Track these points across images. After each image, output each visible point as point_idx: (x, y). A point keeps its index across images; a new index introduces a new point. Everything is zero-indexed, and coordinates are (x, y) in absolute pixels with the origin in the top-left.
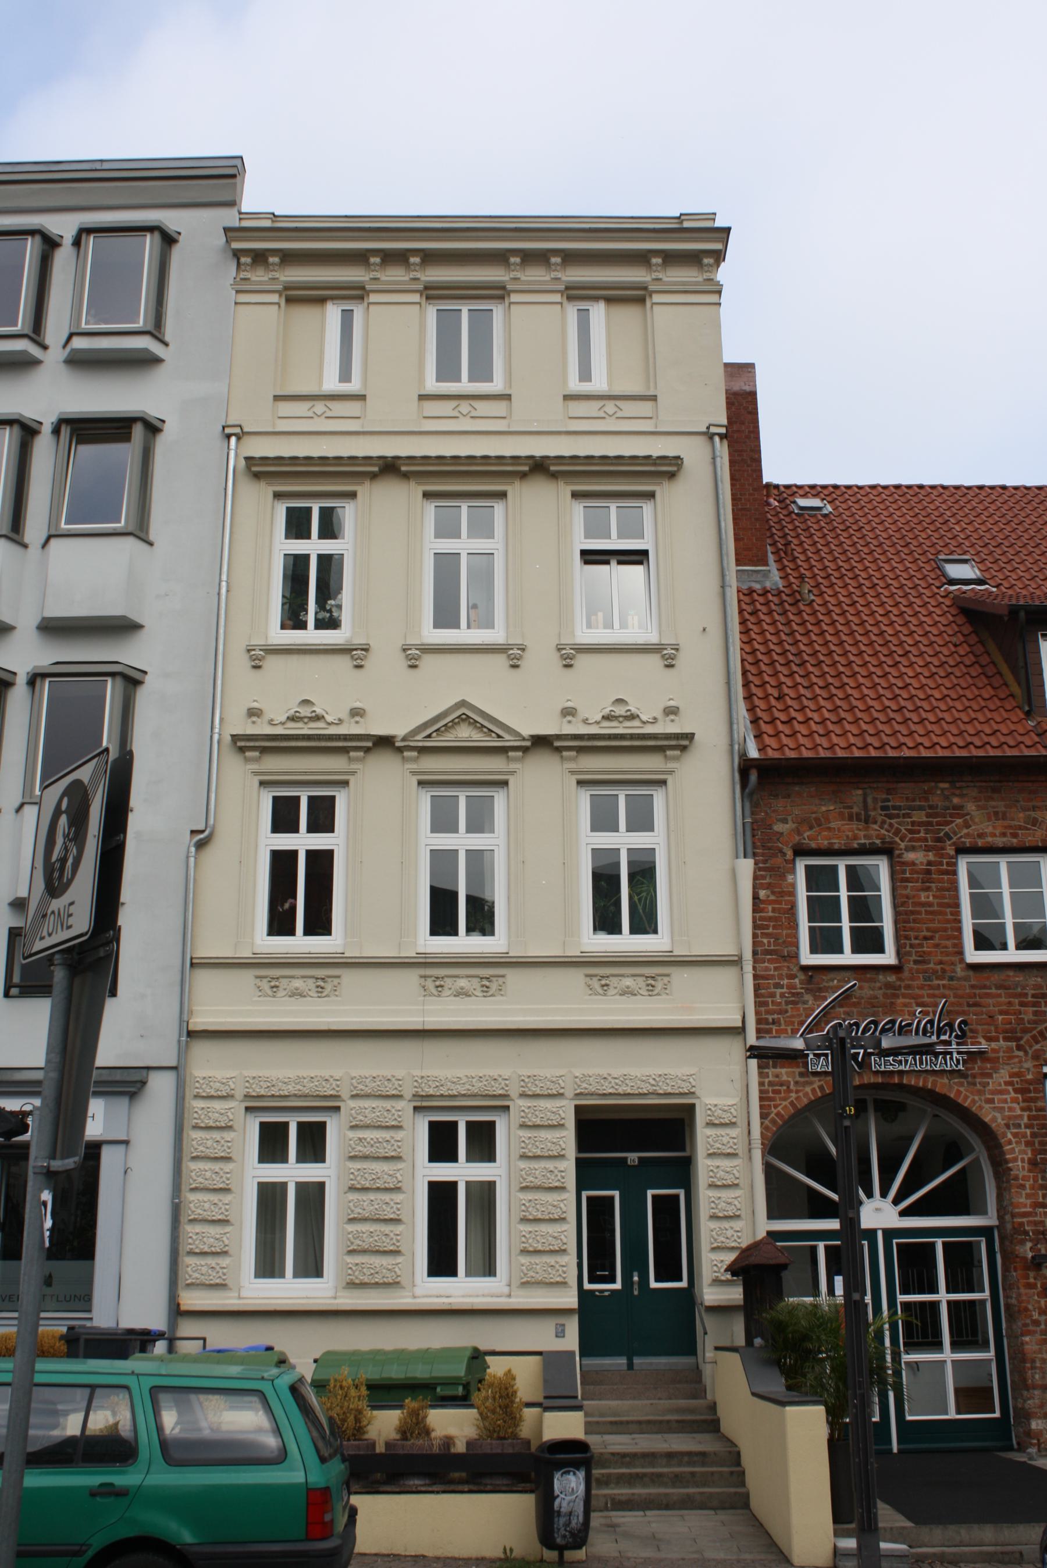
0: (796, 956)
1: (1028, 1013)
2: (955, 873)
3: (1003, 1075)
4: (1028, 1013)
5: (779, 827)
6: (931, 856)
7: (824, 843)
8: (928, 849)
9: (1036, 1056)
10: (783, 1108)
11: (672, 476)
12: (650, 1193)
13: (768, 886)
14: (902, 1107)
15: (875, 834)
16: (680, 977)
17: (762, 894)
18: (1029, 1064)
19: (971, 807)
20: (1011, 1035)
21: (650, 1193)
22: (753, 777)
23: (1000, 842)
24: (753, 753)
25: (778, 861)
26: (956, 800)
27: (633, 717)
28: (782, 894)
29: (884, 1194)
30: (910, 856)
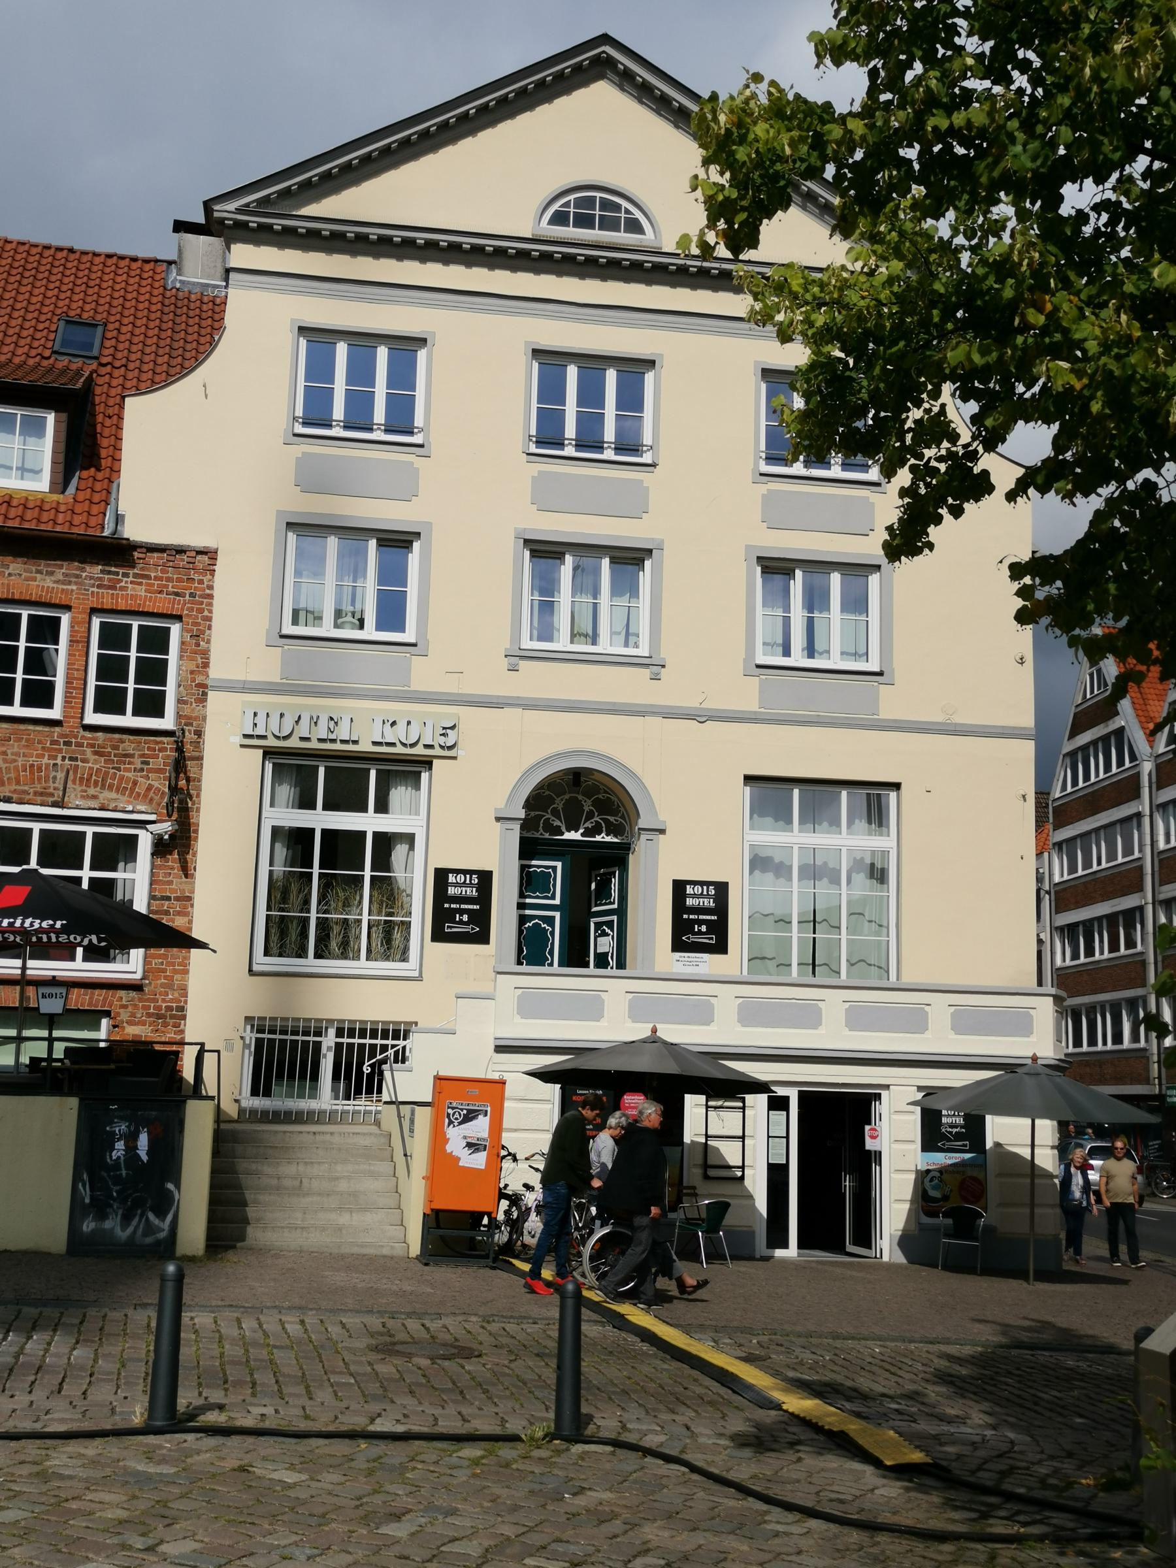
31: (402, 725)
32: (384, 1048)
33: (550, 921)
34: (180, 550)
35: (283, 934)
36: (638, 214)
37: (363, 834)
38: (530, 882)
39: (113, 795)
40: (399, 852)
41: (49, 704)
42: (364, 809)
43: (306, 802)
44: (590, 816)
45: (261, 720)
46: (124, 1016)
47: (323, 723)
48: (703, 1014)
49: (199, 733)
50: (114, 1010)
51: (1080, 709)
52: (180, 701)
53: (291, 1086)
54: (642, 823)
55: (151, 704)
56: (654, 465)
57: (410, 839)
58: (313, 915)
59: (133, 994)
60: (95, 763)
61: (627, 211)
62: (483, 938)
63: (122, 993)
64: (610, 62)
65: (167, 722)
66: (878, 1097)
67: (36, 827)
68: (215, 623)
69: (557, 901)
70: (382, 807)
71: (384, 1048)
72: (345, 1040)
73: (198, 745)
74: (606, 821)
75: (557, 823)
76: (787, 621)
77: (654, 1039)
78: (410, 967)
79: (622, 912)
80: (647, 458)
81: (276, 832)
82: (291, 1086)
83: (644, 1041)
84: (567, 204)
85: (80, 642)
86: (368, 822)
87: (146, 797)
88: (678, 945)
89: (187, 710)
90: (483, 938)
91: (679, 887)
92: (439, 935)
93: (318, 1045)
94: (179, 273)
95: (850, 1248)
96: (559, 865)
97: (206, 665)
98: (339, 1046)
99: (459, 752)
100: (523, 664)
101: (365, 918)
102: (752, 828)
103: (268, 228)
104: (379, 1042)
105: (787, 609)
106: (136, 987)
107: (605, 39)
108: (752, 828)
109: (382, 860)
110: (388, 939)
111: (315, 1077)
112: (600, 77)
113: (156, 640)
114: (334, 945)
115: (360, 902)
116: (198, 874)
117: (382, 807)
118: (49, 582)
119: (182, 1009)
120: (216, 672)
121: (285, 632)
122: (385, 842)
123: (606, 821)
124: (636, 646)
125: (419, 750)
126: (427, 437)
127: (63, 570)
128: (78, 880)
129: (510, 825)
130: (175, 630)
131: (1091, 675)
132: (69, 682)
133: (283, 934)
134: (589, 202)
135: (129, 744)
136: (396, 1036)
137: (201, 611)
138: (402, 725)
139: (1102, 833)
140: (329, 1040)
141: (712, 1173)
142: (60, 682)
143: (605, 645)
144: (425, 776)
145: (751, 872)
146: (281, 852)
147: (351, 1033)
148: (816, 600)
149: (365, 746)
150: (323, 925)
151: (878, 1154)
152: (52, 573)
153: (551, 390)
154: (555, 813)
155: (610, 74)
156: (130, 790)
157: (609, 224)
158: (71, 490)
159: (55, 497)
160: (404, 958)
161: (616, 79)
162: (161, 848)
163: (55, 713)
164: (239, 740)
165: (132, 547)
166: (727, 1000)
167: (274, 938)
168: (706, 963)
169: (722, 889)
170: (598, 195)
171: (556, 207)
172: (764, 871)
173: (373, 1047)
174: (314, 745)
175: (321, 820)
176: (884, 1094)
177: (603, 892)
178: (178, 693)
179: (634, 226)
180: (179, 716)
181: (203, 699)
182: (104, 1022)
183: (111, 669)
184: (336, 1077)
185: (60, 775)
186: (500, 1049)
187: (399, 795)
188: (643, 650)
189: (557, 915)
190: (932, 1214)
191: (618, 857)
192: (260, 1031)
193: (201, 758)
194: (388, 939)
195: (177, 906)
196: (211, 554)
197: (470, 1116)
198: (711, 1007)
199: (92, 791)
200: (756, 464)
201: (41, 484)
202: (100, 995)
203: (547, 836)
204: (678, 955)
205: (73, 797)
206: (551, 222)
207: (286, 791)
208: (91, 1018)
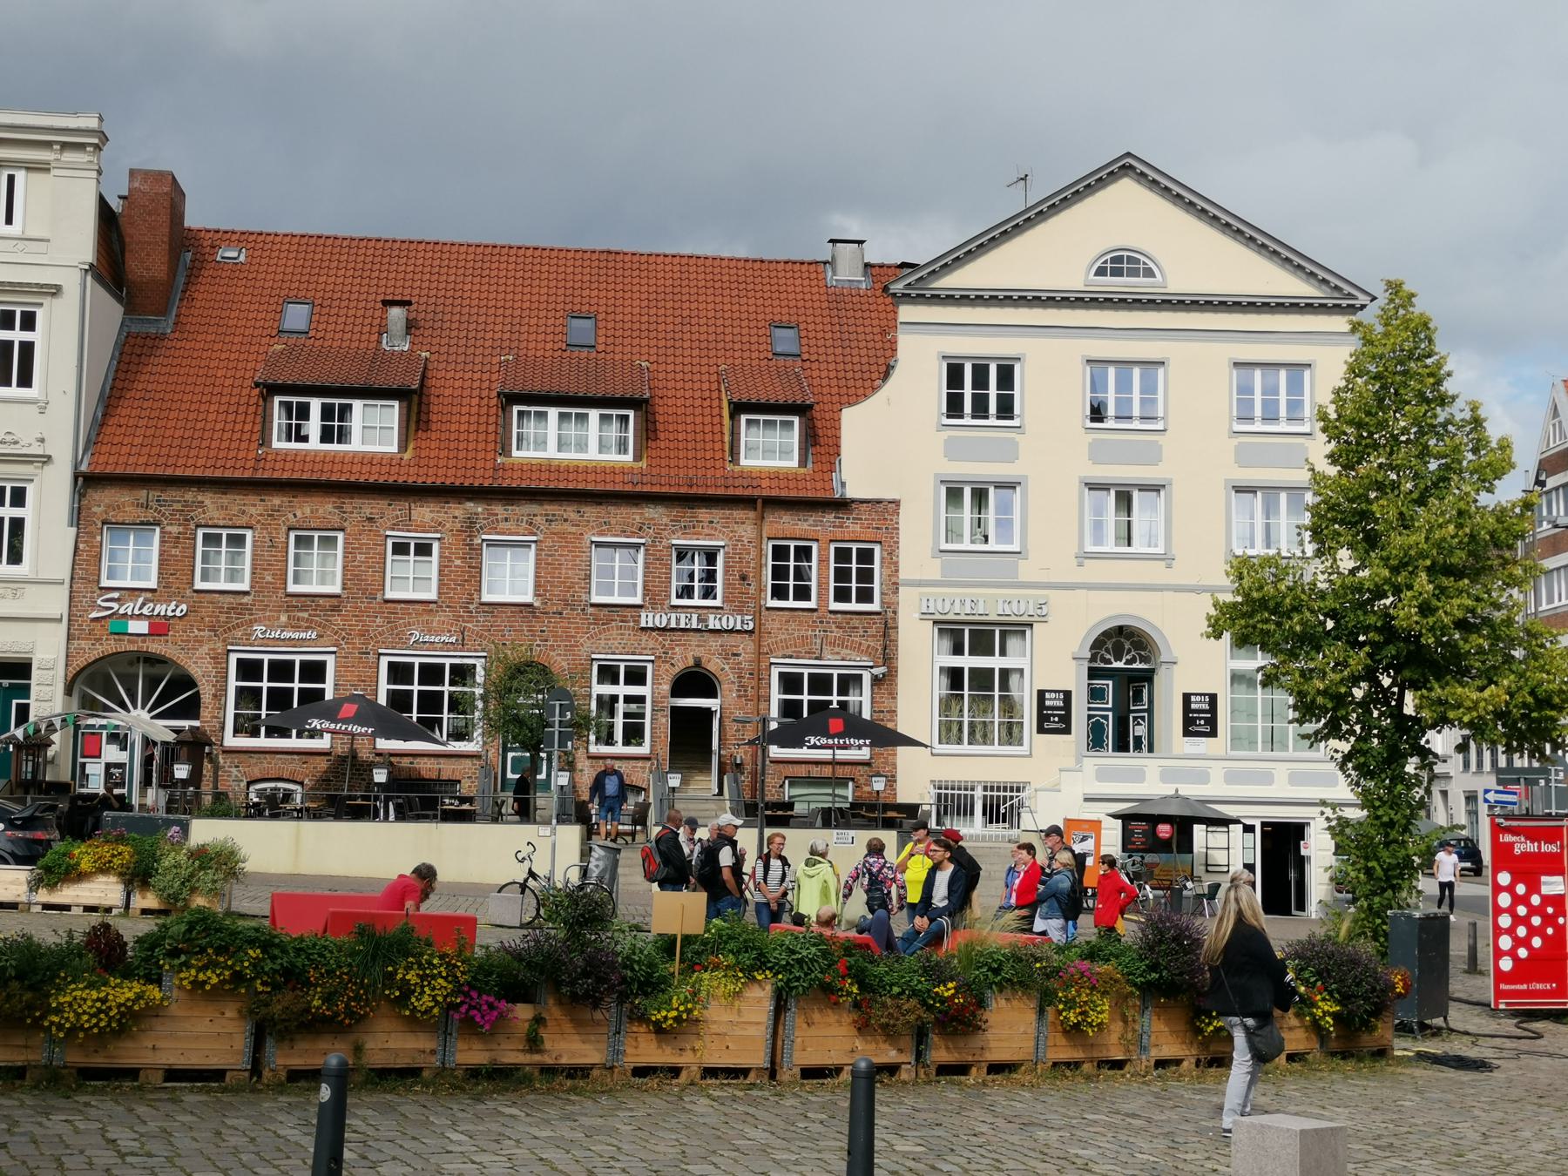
0: (98, 581)
1: (223, 618)
2: (195, 539)
3: (205, 649)
4: (223, 618)
5: (95, 509)
6: (181, 529)
7: (121, 520)
8: (180, 525)
9: (224, 641)
10: (81, 662)
11: (54, 294)
12: (15, 702)
13: (86, 542)
14: (165, 662)
15: (150, 515)
16: (31, 590)
17: (81, 546)
18: (220, 645)
19: (207, 502)
20: (213, 629)
21: (15, 702)
22: (81, 479)
23: (221, 523)
24: (84, 468)
25: (93, 528)
26: (200, 498)
27: (16, 443)
28: (93, 547)
29: (143, 708)
30: (169, 528)
31: (1015, 604)
32: (1012, 798)
33: (1106, 718)
34: (879, 502)
35: (949, 730)
36: (1151, 265)
37: (992, 670)
38: (1095, 694)
39: (849, 652)
40: (1014, 680)
41: (808, 598)
42: (993, 655)
43: (958, 650)
44: (1129, 652)
45: (931, 604)
46: (862, 781)
47: (968, 603)
48: (1203, 778)
49: (895, 612)
50: (856, 777)
51: (1545, 456)
52: (882, 594)
53: (965, 821)
54: (1163, 659)
55: (865, 596)
56: (1165, 430)
57: (1021, 671)
58: (966, 720)
59: (866, 768)
60: (837, 633)
61: (1144, 263)
62: (1067, 731)
63: (860, 768)
64: (1131, 167)
65: (875, 606)
66: (1308, 824)
67: (806, 672)
68: (901, 545)
69: (1110, 706)
70: (1003, 653)
71: (1012, 798)
72: (989, 793)
73: (894, 619)
74: (1140, 655)
75: (1108, 656)
76: (1252, 525)
77: (1177, 796)
78: (1024, 749)
79: (1150, 711)
80: (1160, 426)
81: (941, 669)
82: (965, 821)
83: (1171, 797)
84: (1106, 262)
85: (823, 561)
86: (995, 662)
87: (868, 652)
88: (1187, 733)
89: (887, 599)
90: (1067, 731)
91: (1187, 698)
92: (1041, 730)
93: (972, 796)
94: (834, 273)
95: (1294, 912)
96: (1110, 683)
97: (897, 571)
98: (985, 797)
99: (1049, 618)
100: (1086, 561)
101: (997, 720)
102: (1232, 658)
103: (923, 296)
104: (1008, 794)
105: (1252, 517)
106: (867, 764)
107: (1129, 154)
108: (1232, 658)
109: (1005, 685)
110: (1010, 733)
111: (972, 814)
112: (1126, 175)
113: (865, 556)
114: (978, 736)
115: (993, 711)
116: (899, 697)
117: (1003, 653)
118: (805, 526)
119: (893, 776)
120: (903, 575)
121: (942, 548)
122: (1005, 673)
123: (1140, 655)
124: (1156, 546)
125: (1025, 619)
126: (1022, 420)
127: (813, 518)
128: (831, 702)
129: (1081, 662)
130: (877, 549)
131: (1554, 425)
132: (819, 585)
133: (949, 730)
134: (1118, 260)
135: (855, 621)
136: (1018, 790)
137: (892, 538)
138: (1015, 604)
139: (1562, 571)
140: (979, 793)
141: (1210, 868)
142: (814, 584)
143: (1138, 547)
144: (1028, 633)
145: (1232, 684)
146: (945, 681)
147: (992, 789)
148: (1270, 510)
149: (993, 617)
150: (972, 725)
151: (1309, 858)
152: (806, 520)
153: (1097, 384)
154: (1107, 651)
155: (1130, 173)
156: (858, 648)
157: (1134, 273)
158: (810, 465)
159: (802, 470)
160: (1020, 743)
161: (1135, 177)
162: (876, 681)
163: (812, 604)
164: (917, 615)
165: (853, 501)
166: (1217, 770)
167: (944, 733)
168: (1202, 745)
169: (1213, 698)
170: (1125, 254)
171: (1099, 264)
172: (1240, 683)
173: (1005, 797)
174: (962, 617)
175: (967, 662)
176: (1312, 822)
177: (1138, 697)
178: (881, 589)
179: (1149, 273)
180: (882, 602)
181: (896, 592)
182: (850, 784)
183: (842, 575)
184: (984, 814)
185: (819, 641)
186: (1086, 800)
187: (1013, 643)
188: (1160, 550)
189: (1110, 714)
190: (1340, 891)
191: (1148, 677)
192: (940, 788)
193: (897, 628)
194: (1010, 733)
195: (888, 716)
196: (896, 503)
197: (1084, 839)
198: (1208, 773)
199: (837, 650)
200: (1231, 426)
201: (793, 463)
202: (848, 769)
203: (1102, 665)
204: (1186, 739)
205: (826, 654)
206: (1097, 274)
207: (947, 644)
208: (843, 782)
